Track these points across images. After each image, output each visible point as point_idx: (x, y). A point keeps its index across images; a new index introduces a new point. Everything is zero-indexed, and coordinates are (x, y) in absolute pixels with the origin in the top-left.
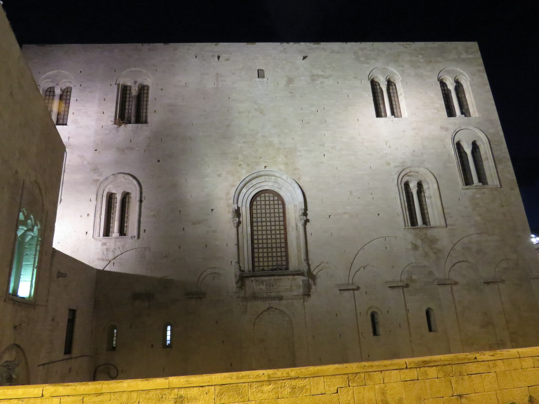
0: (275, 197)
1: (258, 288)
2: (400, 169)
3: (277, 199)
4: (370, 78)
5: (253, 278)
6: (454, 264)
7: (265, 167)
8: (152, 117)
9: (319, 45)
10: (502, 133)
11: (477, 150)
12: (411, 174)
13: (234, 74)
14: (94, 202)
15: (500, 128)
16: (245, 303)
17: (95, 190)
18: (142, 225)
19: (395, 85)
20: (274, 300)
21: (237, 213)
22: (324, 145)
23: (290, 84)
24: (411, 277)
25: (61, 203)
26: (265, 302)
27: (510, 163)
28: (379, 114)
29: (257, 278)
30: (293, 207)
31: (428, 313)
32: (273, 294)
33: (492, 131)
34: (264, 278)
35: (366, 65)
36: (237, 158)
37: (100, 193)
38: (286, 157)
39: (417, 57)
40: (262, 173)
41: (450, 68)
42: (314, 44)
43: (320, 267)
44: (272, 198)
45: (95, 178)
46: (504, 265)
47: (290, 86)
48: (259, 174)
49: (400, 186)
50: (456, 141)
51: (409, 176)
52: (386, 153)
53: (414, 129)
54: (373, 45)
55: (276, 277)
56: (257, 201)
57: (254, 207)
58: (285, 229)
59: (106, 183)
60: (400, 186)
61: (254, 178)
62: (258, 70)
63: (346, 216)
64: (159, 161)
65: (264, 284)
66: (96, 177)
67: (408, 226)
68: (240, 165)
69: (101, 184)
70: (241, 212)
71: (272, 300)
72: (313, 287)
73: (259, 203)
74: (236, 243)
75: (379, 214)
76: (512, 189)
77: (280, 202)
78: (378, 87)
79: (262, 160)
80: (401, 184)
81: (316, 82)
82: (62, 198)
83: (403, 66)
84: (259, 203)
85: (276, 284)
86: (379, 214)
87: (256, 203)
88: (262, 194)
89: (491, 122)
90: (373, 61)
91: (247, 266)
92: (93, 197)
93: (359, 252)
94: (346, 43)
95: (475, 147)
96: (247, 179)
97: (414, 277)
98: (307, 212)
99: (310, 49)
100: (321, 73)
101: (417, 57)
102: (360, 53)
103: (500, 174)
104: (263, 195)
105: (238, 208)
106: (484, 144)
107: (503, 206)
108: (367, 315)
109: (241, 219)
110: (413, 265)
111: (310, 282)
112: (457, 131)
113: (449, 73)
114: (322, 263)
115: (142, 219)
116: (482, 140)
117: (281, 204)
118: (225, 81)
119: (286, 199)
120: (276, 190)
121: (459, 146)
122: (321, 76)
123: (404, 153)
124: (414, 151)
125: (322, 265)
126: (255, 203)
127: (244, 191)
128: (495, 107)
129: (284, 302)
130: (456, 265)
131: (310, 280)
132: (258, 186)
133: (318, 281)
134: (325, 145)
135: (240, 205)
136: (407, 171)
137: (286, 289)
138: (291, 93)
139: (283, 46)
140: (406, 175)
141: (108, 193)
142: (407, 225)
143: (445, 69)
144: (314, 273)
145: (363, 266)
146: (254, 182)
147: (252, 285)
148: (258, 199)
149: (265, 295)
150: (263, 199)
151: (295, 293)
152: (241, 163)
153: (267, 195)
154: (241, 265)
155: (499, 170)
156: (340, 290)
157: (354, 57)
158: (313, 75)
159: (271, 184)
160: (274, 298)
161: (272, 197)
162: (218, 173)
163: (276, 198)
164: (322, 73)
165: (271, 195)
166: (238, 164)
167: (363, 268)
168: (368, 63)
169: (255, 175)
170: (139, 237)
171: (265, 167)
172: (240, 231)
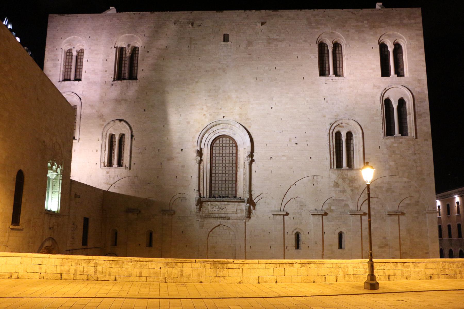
0: (230, 141)
1: (212, 210)
2: (334, 121)
3: (232, 142)
4: (319, 41)
5: (209, 203)
7: (224, 117)
8: (140, 75)
9: (277, 13)
10: (426, 92)
11: (404, 106)
12: (342, 125)
13: (204, 38)
14: (100, 141)
15: (426, 87)
16: (203, 220)
17: (101, 133)
18: (132, 159)
19: (341, 47)
20: (224, 219)
21: (200, 153)
22: (272, 99)
23: (249, 47)
24: (331, 208)
25: (79, 141)
26: (217, 220)
27: (428, 118)
28: (323, 72)
29: (212, 203)
30: (243, 149)
31: (340, 235)
32: (223, 215)
33: (418, 89)
34: (217, 203)
35: (316, 30)
36: (203, 109)
37: (104, 134)
38: (241, 108)
40: (220, 122)
41: (391, 33)
42: (273, 11)
43: (260, 197)
44: (228, 142)
45: (101, 123)
46: (407, 201)
47: (249, 48)
48: (218, 123)
49: (331, 135)
50: (384, 98)
51: (340, 127)
52: (323, 107)
53: (350, 87)
54: (324, 12)
55: (226, 203)
57: (214, 148)
58: (236, 166)
59: (108, 126)
60: (331, 135)
61: (214, 126)
62: (224, 35)
63: (284, 158)
64: (145, 110)
65: (217, 207)
66: (102, 123)
67: (334, 168)
68: (204, 115)
69: (104, 127)
70: (203, 152)
71: (222, 219)
72: (253, 211)
73: (218, 145)
74: (198, 176)
75: (311, 158)
76: (426, 140)
77: (234, 145)
78: (326, 48)
79: (221, 111)
80: (332, 134)
81: (271, 45)
82: (80, 137)
83: (348, 31)
84: (218, 145)
85: (225, 208)
86: (311, 158)
87: (216, 145)
88: (220, 138)
89: (419, 81)
90: (323, 26)
91: (205, 193)
92: (100, 137)
94: (301, 10)
95: (402, 102)
96: (209, 126)
97: (333, 208)
98: (254, 154)
100: (276, 37)
101: (363, 22)
102: (312, 19)
103: (418, 128)
104: (221, 139)
105: (201, 149)
106: (409, 101)
107: (415, 154)
108: (292, 234)
109: (203, 158)
110: (333, 198)
111: (251, 208)
112: (387, 89)
113: (389, 36)
115: (132, 155)
116: (408, 97)
117: (235, 147)
118: (196, 44)
119: (238, 143)
120: (231, 135)
121: (387, 103)
122: (276, 40)
123: (339, 107)
124: (348, 106)
125: (262, 195)
126: (215, 145)
127: (206, 135)
128: (425, 68)
129: (230, 221)
131: (251, 206)
132: (217, 131)
133: (257, 207)
134: (273, 99)
135: (202, 147)
136: (338, 123)
137: (233, 212)
138: (249, 54)
139: (246, 13)
140: (338, 126)
141: (110, 134)
142: (332, 167)
143: (386, 34)
144: (255, 201)
145: (293, 198)
146: (214, 129)
147: (209, 207)
148: (218, 141)
149: (217, 215)
151: (239, 215)
152: (205, 113)
153: (224, 139)
154: (201, 192)
155: (417, 124)
156: (274, 215)
157: (306, 23)
159: (227, 130)
160: (223, 218)
161: (229, 141)
162: (187, 121)
163: (231, 142)
164: (278, 37)
165: (228, 139)
166: (203, 114)
167: (293, 199)
168: (318, 28)
169: (214, 124)
170: (130, 169)
171: (224, 117)
172: (201, 167)
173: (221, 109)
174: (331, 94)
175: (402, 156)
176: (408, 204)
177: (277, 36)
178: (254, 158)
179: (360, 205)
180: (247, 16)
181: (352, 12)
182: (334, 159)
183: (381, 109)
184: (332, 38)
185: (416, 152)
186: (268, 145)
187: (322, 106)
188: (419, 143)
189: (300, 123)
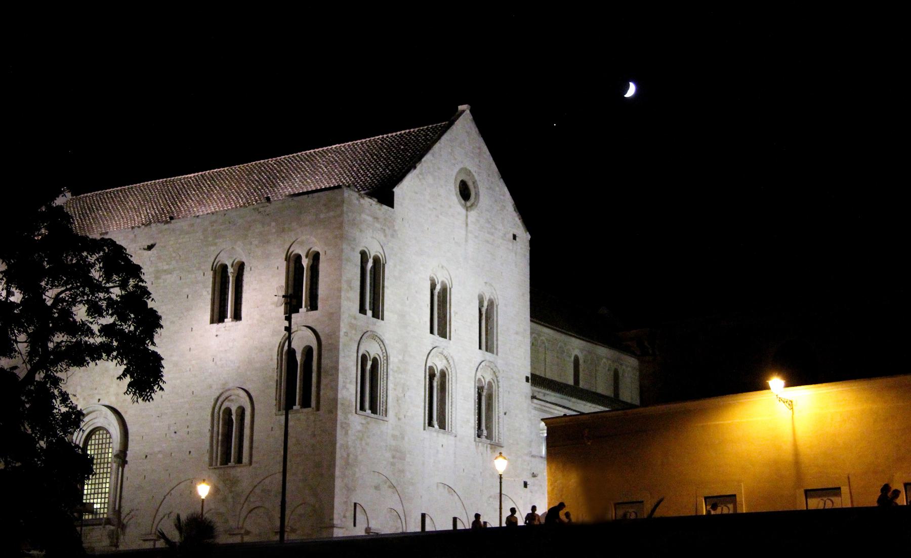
4: (216, 265)
6: (252, 510)
12: (232, 397)
35: (212, 248)
39: (269, 225)
43: (130, 516)
51: (229, 401)
52: (211, 372)
55: (91, 527)
56: (92, 440)
63: (160, 456)
72: (122, 537)
73: (93, 442)
75: (190, 452)
79: (97, 391)
86: (190, 452)
88: (97, 431)
93: (167, 497)
99: (161, 232)
107: (314, 435)
110: (213, 511)
111: (119, 532)
114: (132, 510)
125: (133, 513)
130: (254, 511)
133: (128, 530)
140: (227, 400)
142: (214, 464)
144: (125, 522)
150: (97, 437)
157: (202, 237)
158: (158, 271)
163: (108, 436)
167: (167, 516)
168: (216, 244)
173: (96, 389)
174: (222, 351)
175: (297, 440)
176: (301, 515)
177: (167, 264)
178: (127, 459)
179: (241, 520)
180: (135, 235)
181: (258, 210)
182: (217, 452)
183: (277, 369)
184: (231, 258)
185: (316, 433)
186: (144, 438)
187: (210, 371)
188: (320, 419)
189: (182, 400)
